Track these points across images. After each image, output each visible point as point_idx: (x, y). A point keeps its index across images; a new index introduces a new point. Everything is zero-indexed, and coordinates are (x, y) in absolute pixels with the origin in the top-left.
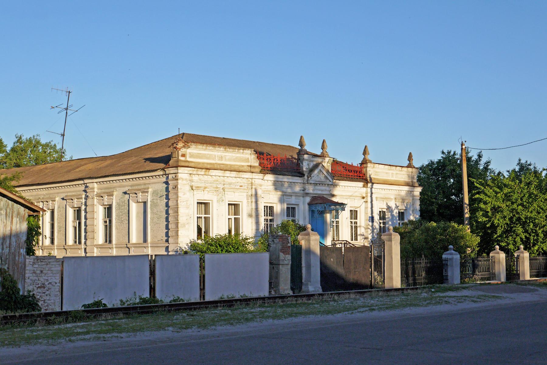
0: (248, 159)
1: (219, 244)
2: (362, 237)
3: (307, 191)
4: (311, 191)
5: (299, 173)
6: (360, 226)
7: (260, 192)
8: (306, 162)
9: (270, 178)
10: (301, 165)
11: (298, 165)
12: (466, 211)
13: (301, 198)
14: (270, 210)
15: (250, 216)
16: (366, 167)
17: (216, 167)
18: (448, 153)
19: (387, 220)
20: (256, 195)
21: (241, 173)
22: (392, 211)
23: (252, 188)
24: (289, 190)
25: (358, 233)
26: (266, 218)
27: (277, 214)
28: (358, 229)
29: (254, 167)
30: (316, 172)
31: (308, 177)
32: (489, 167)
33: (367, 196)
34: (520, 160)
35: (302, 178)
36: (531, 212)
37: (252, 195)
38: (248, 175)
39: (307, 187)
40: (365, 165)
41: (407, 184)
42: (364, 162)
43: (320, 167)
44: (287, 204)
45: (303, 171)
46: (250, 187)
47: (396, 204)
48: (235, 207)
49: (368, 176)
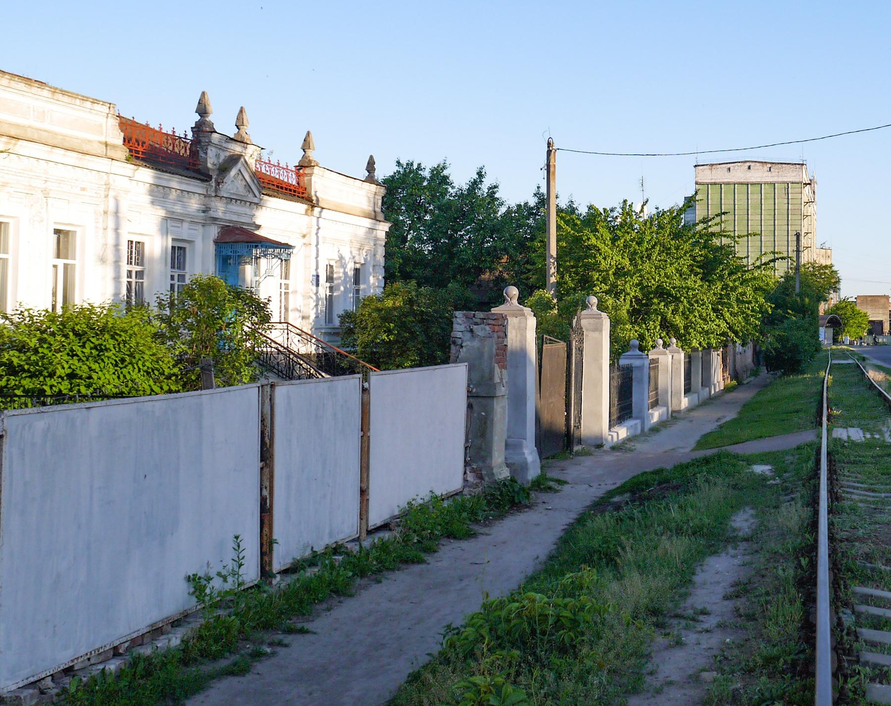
0: (101, 126)
1: (73, 330)
2: (297, 314)
3: (212, 214)
4: (220, 214)
5: (198, 171)
6: (295, 292)
7: (123, 209)
8: (213, 149)
9: (146, 175)
10: (202, 154)
11: (194, 154)
12: (553, 270)
13: (200, 227)
14: (137, 251)
15: (103, 260)
16: (311, 175)
17: (29, 135)
18: (407, 164)
19: (336, 282)
20: (117, 213)
21: (87, 157)
22: (344, 266)
23: (107, 196)
24: (178, 209)
25: (290, 307)
26: (129, 268)
27: (151, 259)
28: (291, 296)
29: (114, 147)
30: (233, 172)
31: (218, 184)
32: (496, 196)
33: (310, 233)
34: (538, 188)
35: (205, 185)
36: (735, 281)
37: (105, 213)
38: (103, 164)
39: (213, 204)
40: (307, 171)
41: (368, 216)
42: (305, 165)
43: (239, 165)
44: (173, 240)
45: (208, 169)
46: (103, 194)
47: (351, 252)
48: (63, 239)
49: (313, 193)
